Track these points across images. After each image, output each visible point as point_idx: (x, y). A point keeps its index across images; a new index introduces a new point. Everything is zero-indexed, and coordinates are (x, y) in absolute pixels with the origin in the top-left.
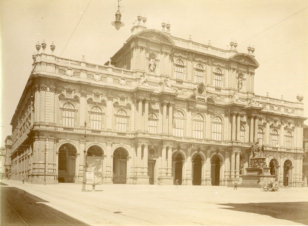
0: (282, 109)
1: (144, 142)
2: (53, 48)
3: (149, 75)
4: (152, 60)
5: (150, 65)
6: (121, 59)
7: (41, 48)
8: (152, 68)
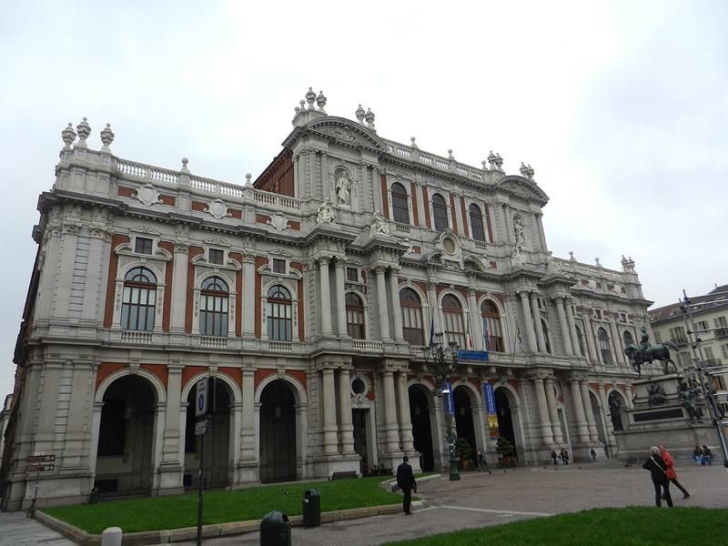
0: (605, 285)
1: (339, 362)
2: (107, 137)
3: (338, 210)
4: (342, 179)
5: (338, 190)
6: (277, 176)
7: (78, 138)
8: (342, 194)
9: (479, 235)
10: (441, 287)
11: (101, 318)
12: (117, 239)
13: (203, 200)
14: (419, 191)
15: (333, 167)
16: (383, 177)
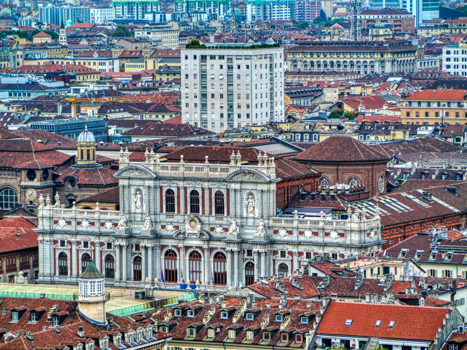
5: (136, 202)
9: (220, 210)
10: (187, 248)
11: (53, 272)
12: (55, 242)
13: (80, 220)
14: (182, 191)
15: (133, 190)
16: (161, 188)
